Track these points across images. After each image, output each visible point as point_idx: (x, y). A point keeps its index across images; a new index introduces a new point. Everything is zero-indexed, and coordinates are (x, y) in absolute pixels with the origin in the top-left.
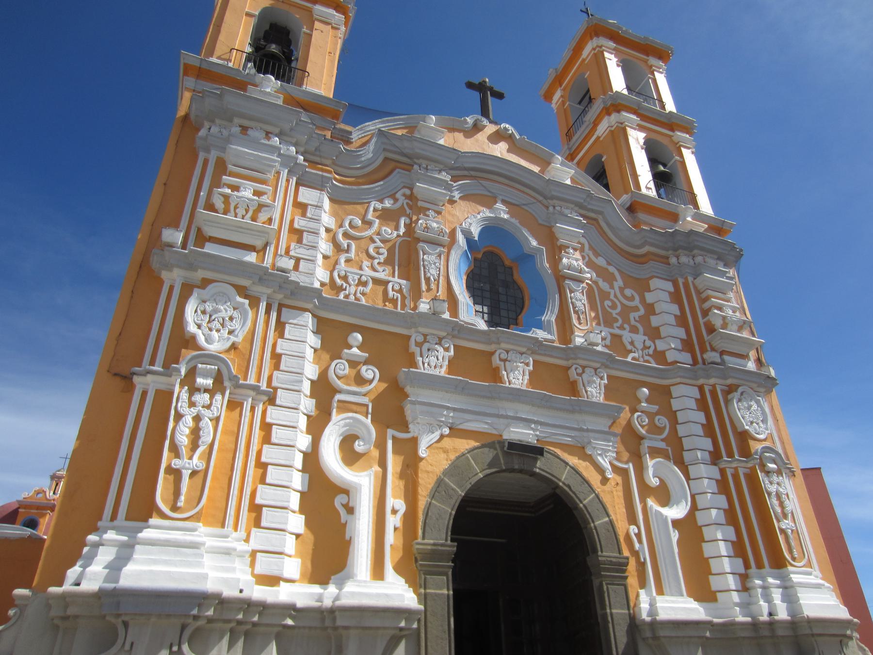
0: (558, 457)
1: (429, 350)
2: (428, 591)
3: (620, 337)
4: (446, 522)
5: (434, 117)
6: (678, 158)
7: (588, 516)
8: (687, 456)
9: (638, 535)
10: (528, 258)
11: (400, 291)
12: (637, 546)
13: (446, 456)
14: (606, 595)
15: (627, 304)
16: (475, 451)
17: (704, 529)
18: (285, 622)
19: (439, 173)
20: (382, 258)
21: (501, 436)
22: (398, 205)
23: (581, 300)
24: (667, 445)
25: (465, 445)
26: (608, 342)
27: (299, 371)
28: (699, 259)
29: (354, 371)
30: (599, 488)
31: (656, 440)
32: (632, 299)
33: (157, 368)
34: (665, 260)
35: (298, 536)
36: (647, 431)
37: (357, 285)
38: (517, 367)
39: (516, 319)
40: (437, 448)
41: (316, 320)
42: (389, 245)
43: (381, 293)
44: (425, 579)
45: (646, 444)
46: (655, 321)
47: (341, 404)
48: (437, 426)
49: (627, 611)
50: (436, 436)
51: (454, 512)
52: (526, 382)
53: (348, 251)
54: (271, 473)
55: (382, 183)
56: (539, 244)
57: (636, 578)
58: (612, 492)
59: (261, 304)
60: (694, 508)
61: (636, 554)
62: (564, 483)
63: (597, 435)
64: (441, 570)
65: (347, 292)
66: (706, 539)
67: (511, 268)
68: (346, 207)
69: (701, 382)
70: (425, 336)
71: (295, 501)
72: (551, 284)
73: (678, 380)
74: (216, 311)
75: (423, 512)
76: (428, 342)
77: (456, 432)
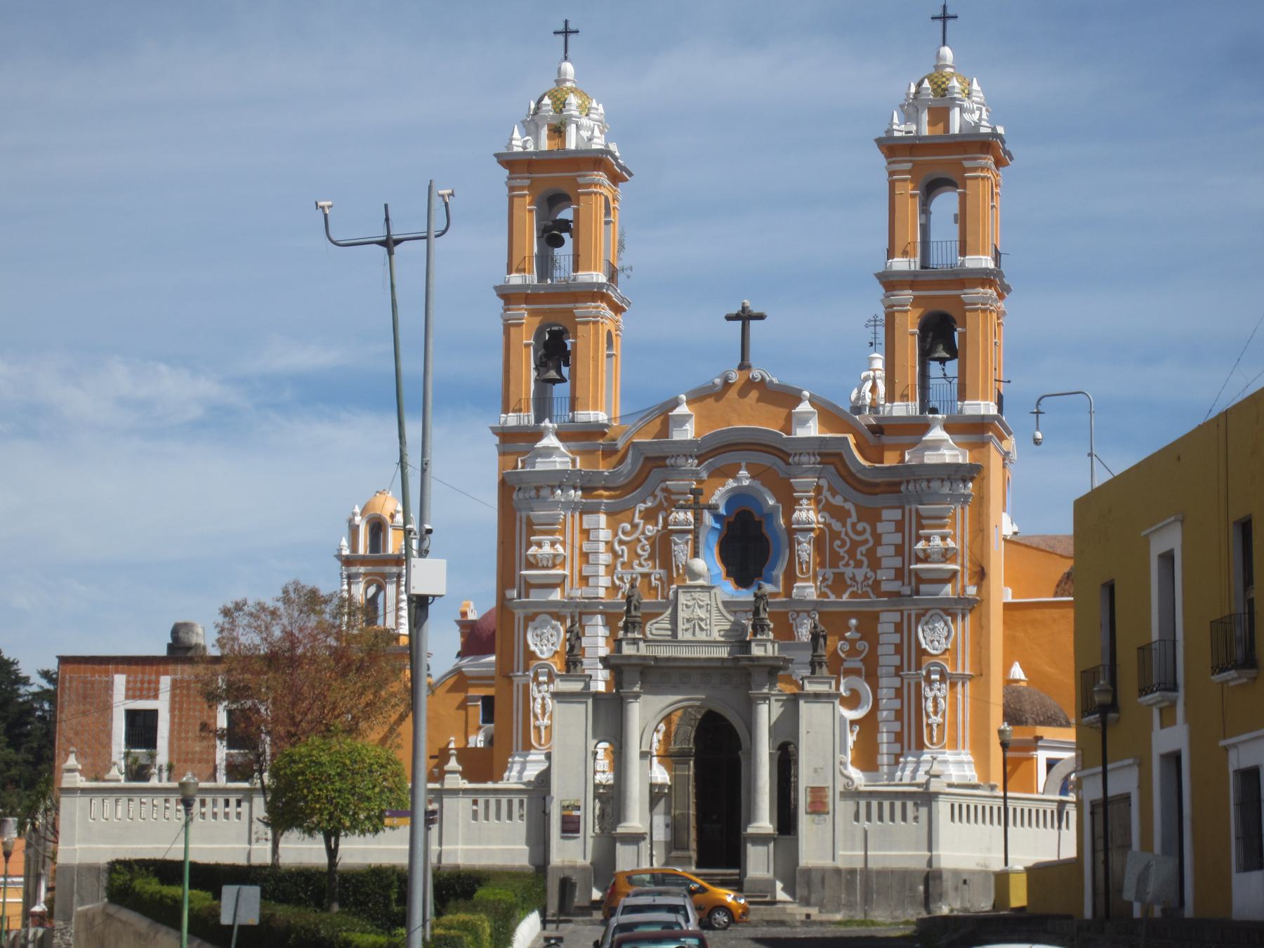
3: (842, 574)
10: (770, 516)
11: (660, 579)
20: (646, 554)
26: (830, 582)
31: (855, 661)
33: (520, 673)
36: (847, 656)
41: (604, 617)
42: (652, 540)
45: (846, 665)
72: (784, 538)
74: (543, 633)
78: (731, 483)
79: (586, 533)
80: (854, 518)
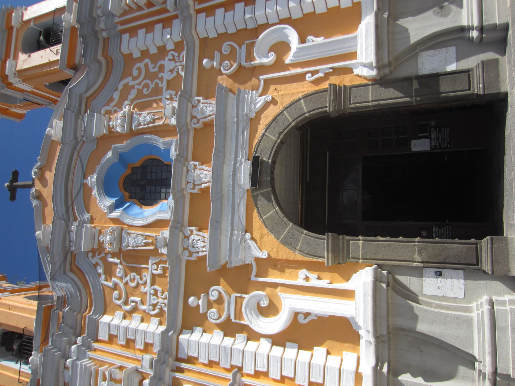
0: (259, 142)
1: (193, 247)
2: (361, 257)
3: (168, 82)
4: (312, 238)
5: (37, 233)
6: (32, 24)
7: (301, 118)
8: (251, 26)
9: (313, 73)
10: (122, 158)
11: (157, 264)
12: (321, 75)
13: (265, 236)
14: (358, 105)
15: (145, 72)
16: (260, 211)
17: (305, 12)
18: (386, 373)
19: (73, 232)
20: (138, 277)
21: (248, 190)
22: (100, 262)
23: (145, 117)
24: (244, 44)
25: (257, 221)
26: (173, 93)
27: (218, 348)
28: (99, 12)
29: (215, 305)
30: (279, 107)
32: (139, 69)
34: (106, 40)
35: (328, 353)
37: (157, 297)
38: (197, 175)
39: (167, 165)
40: (261, 242)
41: (184, 331)
42: (127, 271)
43: (160, 279)
44: (352, 258)
45: (244, 63)
46: (153, 50)
47: (237, 317)
48: (245, 243)
49: (370, 87)
50: (251, 243)
51: (305, 232)
52: (207, 168)
53: (136, 303)
54: (287, 373)
55: (87, 276)
56: (110, 150)
57: (345, 76)
58: (282, 95)
59: (176, 376)
60: (288, 21)
61: (327, 76)
62: (278, 138)
63: (241, 109)
64: (345, 246)
65: (163, 305)
66: (313, 10)
67: (133, 168)
68: (107, 301)
69: (192, 12)
70: (184, 249)
71: (304, 355)
72: (137, 140)
73: (193, 32)
75: (306, 257)
76: (188, 246)
77: (248, 229)
78: (95, 192)
79: (112, 339)
80: (129, 79)
